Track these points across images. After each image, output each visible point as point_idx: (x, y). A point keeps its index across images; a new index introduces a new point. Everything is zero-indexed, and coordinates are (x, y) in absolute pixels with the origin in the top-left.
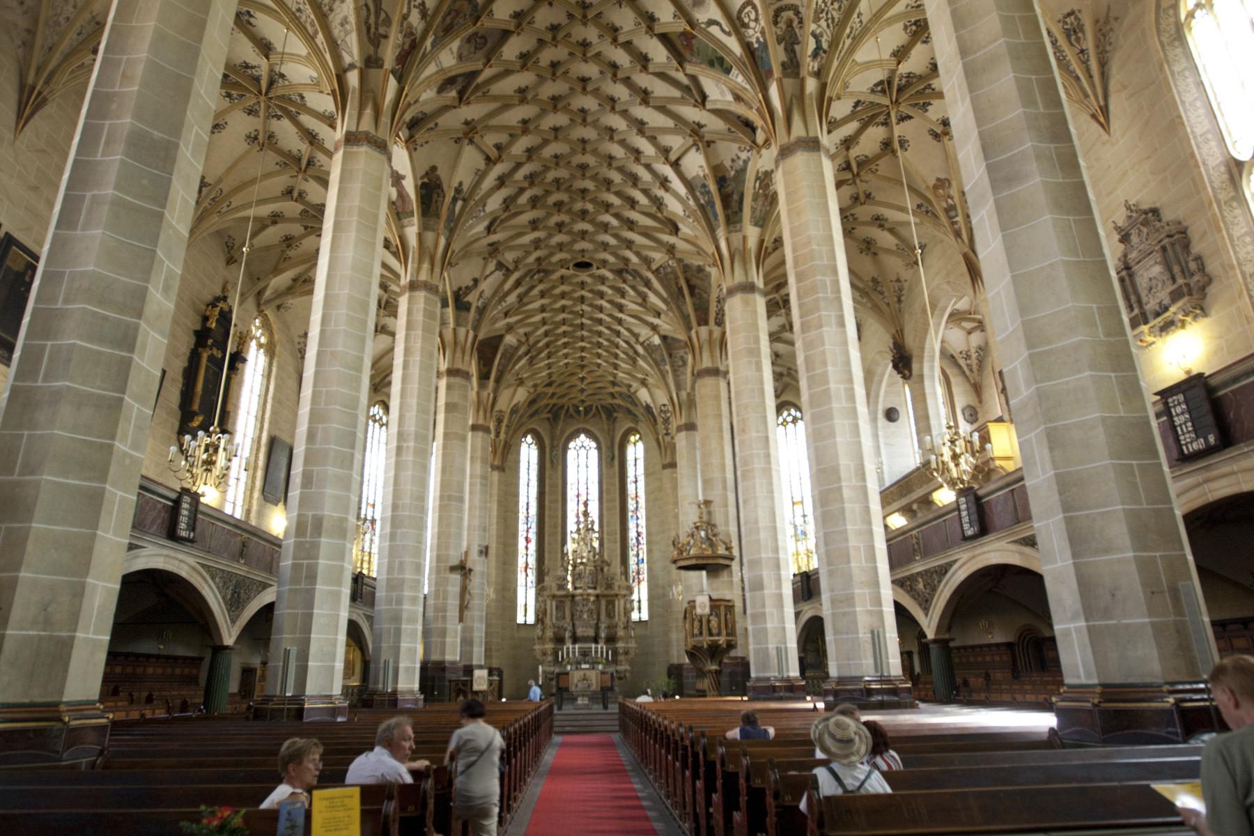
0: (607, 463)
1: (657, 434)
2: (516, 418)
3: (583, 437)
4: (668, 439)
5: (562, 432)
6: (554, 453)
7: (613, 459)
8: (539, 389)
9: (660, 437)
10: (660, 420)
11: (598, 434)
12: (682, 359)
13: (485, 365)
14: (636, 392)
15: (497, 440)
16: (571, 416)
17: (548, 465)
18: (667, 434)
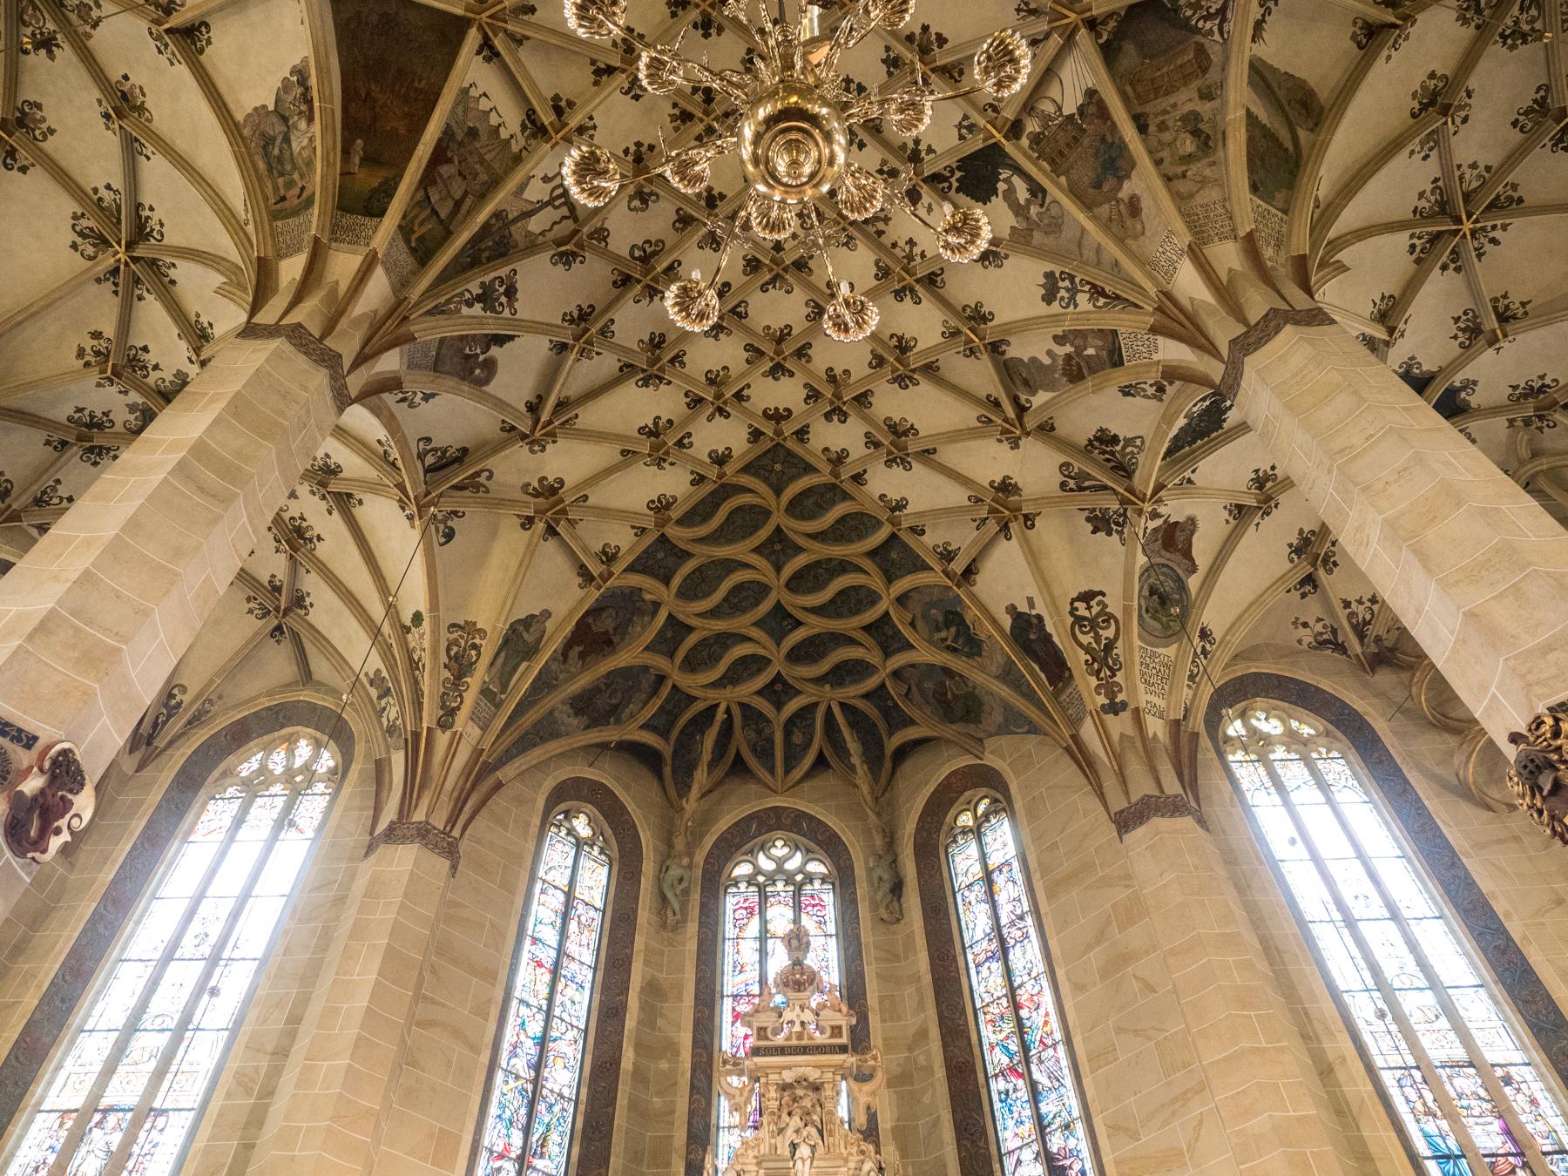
0: (874, 906)
1: (1075, 723)
2: (526, 676)
3: (779, 850)
4: (1119, 725)
5: (705, 821)
6: (675, 872)
7: (897, 888)
8: (621, 579)
9: (1088, 731)
10: (1076, 659)
11: (833, 822)
12: (1193, 124)
13: (370, 160)
14: (969, 572)
15: (442, 739)
16: (739, 768)
17: (645, 914)
18: (1114, 708)
